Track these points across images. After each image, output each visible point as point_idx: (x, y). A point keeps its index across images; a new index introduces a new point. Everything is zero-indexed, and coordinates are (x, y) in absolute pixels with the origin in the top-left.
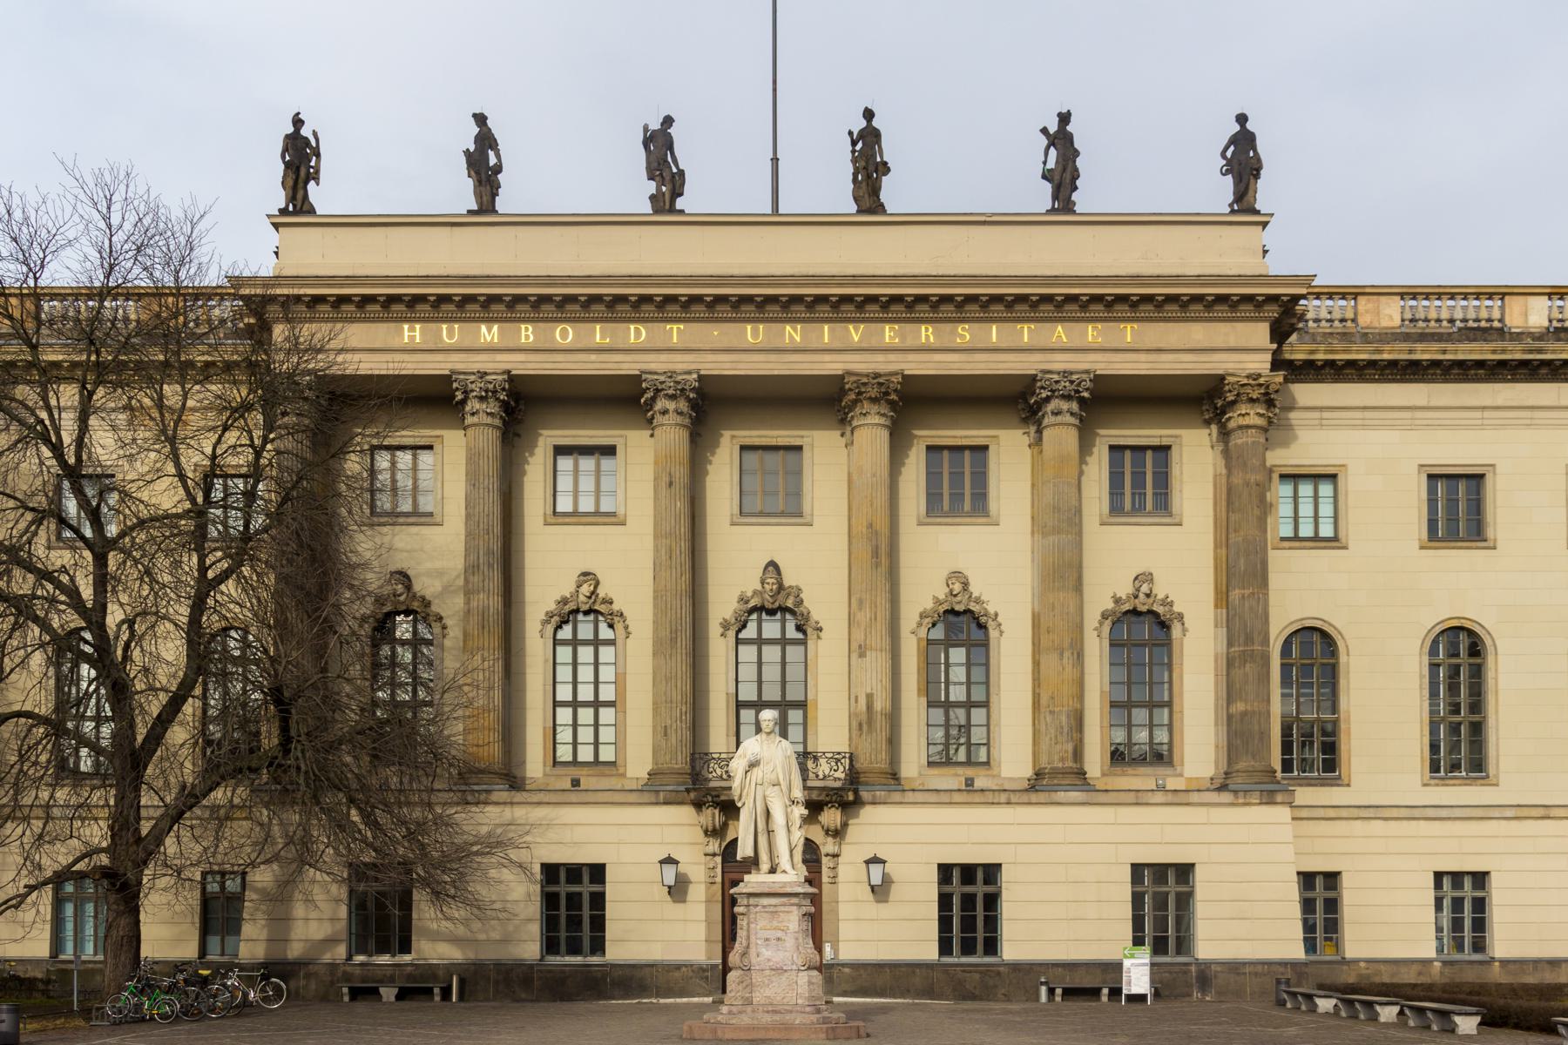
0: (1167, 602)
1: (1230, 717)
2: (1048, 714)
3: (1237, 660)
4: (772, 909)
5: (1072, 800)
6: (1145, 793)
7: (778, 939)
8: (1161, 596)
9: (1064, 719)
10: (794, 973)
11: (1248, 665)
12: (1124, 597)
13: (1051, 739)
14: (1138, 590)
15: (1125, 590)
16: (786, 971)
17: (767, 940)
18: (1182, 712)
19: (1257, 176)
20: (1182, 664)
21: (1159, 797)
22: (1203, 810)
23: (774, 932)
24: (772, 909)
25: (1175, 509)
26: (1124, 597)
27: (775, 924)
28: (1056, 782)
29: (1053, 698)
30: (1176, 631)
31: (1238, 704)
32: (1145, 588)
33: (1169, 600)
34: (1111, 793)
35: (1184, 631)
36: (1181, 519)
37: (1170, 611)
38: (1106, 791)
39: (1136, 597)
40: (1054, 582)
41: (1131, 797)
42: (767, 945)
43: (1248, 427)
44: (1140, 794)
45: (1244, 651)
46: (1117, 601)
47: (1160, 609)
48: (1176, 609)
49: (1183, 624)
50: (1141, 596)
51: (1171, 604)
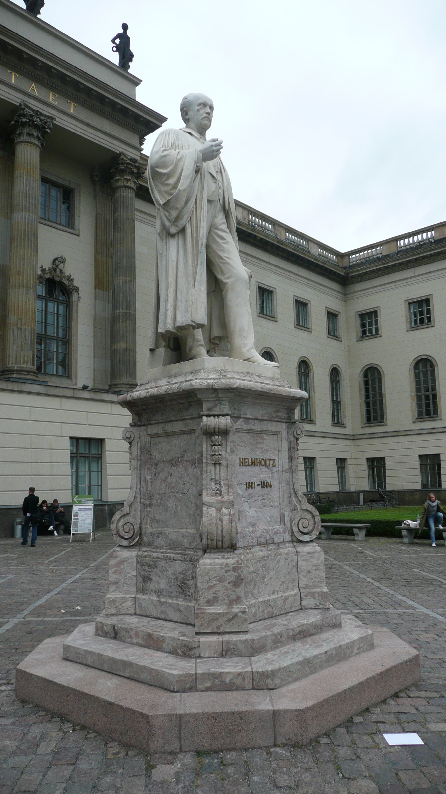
0: (70, 279)
1: (114, 352)
2: (16, 329)
3: (121, 318)
4: (256, 426)
5: (34, 391)
6: (78, 391)
7: (265, 485)
8: (67, 274)
9: (27, 333)
10: (288, 549)
11: (128, 321)
12: (47, 270)
13: (17, 347)
14: (57, 266)
15: (48, 265)
16: (279, 544)
17: (250, 485)
18: (76, 346)
19: (131, 61)
20: (77, 318)
21: (85, 395)
22: (109, 405)
23: (256, 469)
24: (256, 426)
25: (76, 226)
26: (47, 270)
27: (258, 455)
28: (23, 376)
29: (21, 319)
30: (74, 297)
31: (122, 344)
32: (61, 266)
33: (72, 277)
34: (58, 388)
35: (79, 298)
36: (79, 233)
37: (72, 284)
38: (56, 387)
39: (55, 270)
40: (24, 242)
41: (69, 393)
42: (250, 497)
43: (129, 187)
44: (75, 391)
45: (126, 313)
46: (43, 270)
47: (66, 282)
48: (75, 284)
49: (78, 294)
50: (58, 271)
51: (72, 280)
